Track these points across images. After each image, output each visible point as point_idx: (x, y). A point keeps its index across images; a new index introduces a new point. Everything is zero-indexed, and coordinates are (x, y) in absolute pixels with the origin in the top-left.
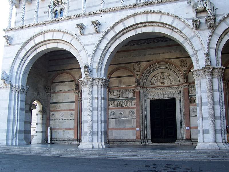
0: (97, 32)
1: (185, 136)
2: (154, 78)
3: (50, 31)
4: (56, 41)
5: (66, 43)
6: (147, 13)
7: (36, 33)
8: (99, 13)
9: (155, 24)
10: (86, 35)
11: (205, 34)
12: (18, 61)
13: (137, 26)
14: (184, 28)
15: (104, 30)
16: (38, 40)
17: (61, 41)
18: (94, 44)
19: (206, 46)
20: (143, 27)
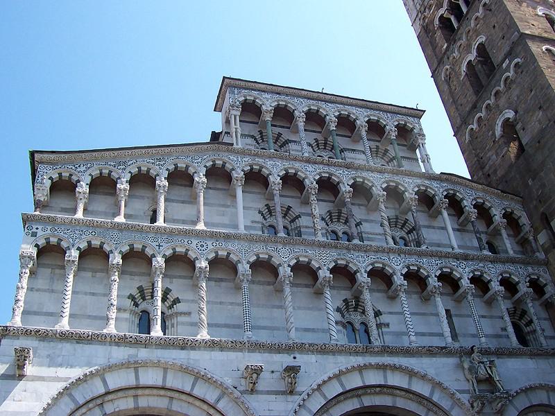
0: (291, 393)
3: (157, 364)
4: (169, 394)
5: (198, 403)
6: (383, 368)
7: (113, 361)
8: (290, 349)
10: (262, 393)
14: (452, 408)
15: (303, 385)
17: (184, 397)
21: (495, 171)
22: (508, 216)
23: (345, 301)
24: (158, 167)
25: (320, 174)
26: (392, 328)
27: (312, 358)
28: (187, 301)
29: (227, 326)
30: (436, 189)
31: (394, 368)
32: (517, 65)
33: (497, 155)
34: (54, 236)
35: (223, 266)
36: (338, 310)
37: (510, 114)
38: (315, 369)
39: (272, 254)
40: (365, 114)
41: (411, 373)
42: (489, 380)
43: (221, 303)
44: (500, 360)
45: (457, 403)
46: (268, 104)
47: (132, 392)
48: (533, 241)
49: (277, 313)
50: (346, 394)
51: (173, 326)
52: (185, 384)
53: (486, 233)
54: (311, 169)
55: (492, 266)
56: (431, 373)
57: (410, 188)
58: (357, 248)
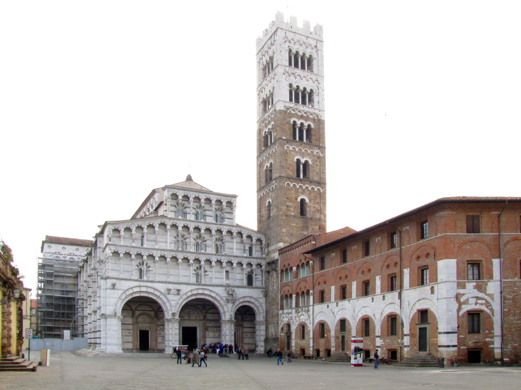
0: (178, 294)
2: (185, 314)
13: (198, 294)
15: (181, 293)
18: (176, 301)
20: (200, 295)
21: (263, 217)
22: (259, 240)
23: (197, 268)
26: (209, 276)
27: (184, 286)
31: (206, 289)
32: (276, 185)
35: (163, 257)
36: (195, 270)
37: (271, 202)
38: (185, 289)
41: (211, 291)
44: (238, 289)
49: (177, 271)
53: (250, 244)
56: (217, 291)
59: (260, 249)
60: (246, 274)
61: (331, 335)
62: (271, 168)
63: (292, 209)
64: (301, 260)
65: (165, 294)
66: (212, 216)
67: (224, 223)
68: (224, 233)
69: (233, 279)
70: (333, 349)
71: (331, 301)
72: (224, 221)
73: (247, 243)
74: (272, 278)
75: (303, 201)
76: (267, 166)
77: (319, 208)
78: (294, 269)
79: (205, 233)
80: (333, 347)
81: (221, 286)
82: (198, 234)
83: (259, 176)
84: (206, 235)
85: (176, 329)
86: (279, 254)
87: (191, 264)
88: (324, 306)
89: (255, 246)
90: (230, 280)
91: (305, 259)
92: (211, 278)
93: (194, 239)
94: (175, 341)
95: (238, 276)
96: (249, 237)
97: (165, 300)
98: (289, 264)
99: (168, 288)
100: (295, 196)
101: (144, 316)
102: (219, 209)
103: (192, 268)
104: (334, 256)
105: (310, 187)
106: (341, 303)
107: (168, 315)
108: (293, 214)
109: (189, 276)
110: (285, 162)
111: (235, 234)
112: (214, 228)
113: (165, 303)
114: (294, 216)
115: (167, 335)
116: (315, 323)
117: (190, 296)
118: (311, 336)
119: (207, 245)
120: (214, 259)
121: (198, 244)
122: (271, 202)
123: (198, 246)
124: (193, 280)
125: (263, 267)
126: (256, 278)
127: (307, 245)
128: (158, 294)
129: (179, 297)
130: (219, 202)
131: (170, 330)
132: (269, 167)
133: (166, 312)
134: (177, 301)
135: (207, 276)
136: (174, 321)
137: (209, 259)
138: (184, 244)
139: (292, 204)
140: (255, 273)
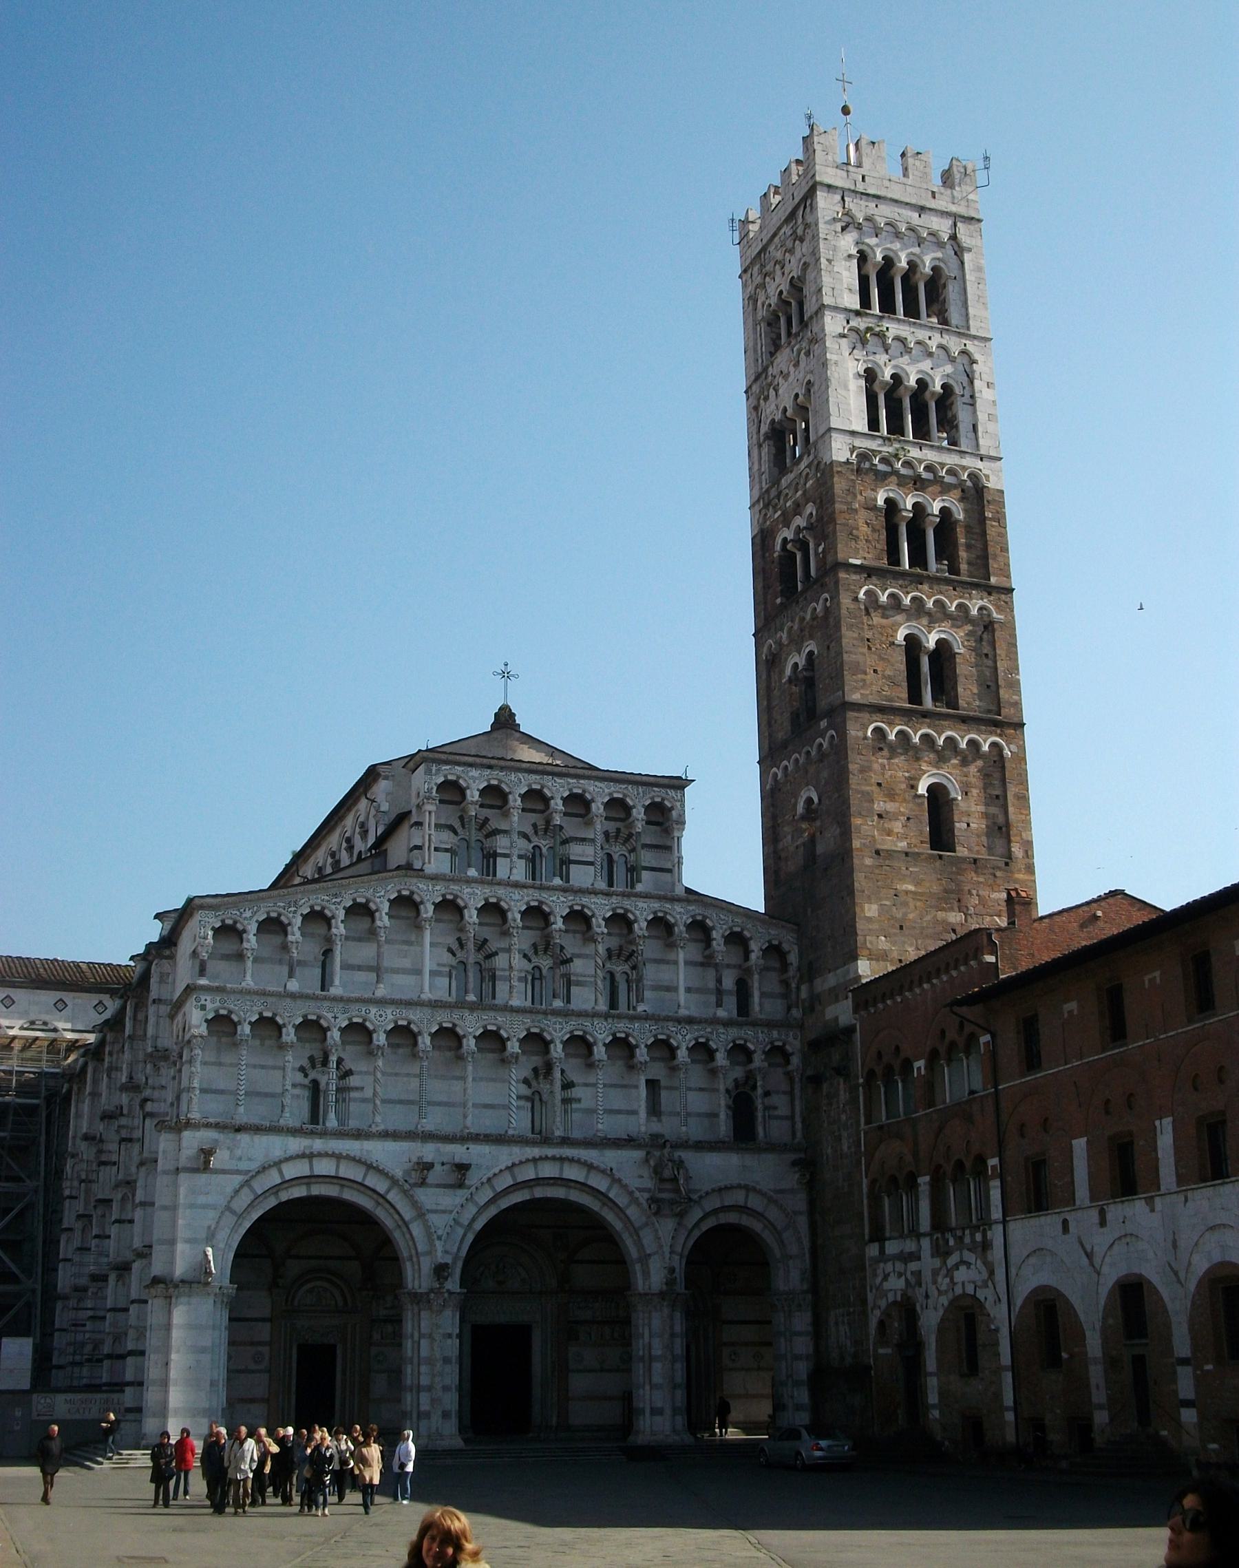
0: (461, 1185)
1: (554, 1419)
5: (370, 1193)
7: (289, 1153)
9: (572, 1184)
10: (431, 1186)
11: (667, 1226)
12: (230, 1219)
13: (539, 1181)
14: (628, 1206)
15: (473, 1178)
16: (291, 1171)
17: (355, 1186)
18: (451, 1212)
19: (667, 1250)
20: (548, 1184)
22: (774, 951)
23: (535, 1070)
24: (333, 907)
25: (528, 903)
27: (486, 1149)
28: (360, 1073)
29: (401, 1102)
30: (678, 916)
33: (793, 838)
34: (225, 1008)
35: (404, 1034)
36: (526, 1081)
37: (816, 800)
39: (457, 1022)
40: (606, 791)
41: (590, 1167)
42: (675, 1180)
43: (396, 1074)
44: (698, 1155)
45: (634, 1201)
46: (475, 782)
47: (306, 1180)
48: (794, 990)
49: (457, 1086)
50: (517, 1186)
51: (344, 1100)
52: (354, 1172)
53: (740, 967)
54: (517, 897)
55: (722, 1031)
57: (642, 912)
58: (556, 1013)
59: (777, 989)
60: (727, 1091)
61: (1086, 1354)
62: (813, 670)
63: (897, 827)
64: (943, 1032)
65: (407, 1187)
66: (591, 863)
67: (639, 888)
68: (640, 927)
69: (679, 1114)
70: (1101, 1418)
71: (1078, 1203)
72: (639, 881)
73: (728, 966)
74: (831, 1104)
75: (936, 792)
76: (796, 665)
77: (1001, 820)
78: (919, 1069)
79: (566, 931)
80: (1101, 1407)
81: (629, 1142)
82: (538, 933)
83: (765, 703)
84: (571, 935)
85: (450, 1336)
86: (856, 1009)
87: (512, 1055)
88: (1048, 1223)
89: (760, 974)
90: (664, 1118)
91: (961, 1026)
92: (591, 1111)
93: (525, 956)
94: (446, 1389)
95: (697, 1102)
96: (736, 939)
97: (408, 1214)
98: (897, 1048)
99: (421, 1158)
100: (907, 774)
101: (318, 1283)
102: (617, 837)
103: (518, 1072)
104: (1075, 1012)
105: (962, 738)
106: (1115, 1211)
107: (418, 1277)
108: (902, 845)
109: (507, 1107)
110: (865, 650)
111: (680, 929)
112: (600, 909)
113: (406, 1224)
114: (907, 854)
115: (412, 1363)
116: (1019, 1302)
117: (507, 1191)
118: (1006, 1358)
119: (573, 978)
120: (601, 1033)
121: (537, 975)
122: (816, 800)
123: (537, 983)
124: (520, 1122)
125: (795, 1060)
126: (766, 1108)
127: (962, 968)
128: (381, 1186)
129: (460, 1196)
130: (618, 807)
131: (424, 1343)
132: (804, 669)
133: (408, 1264)
134: (452, 1216)
135: (575, 1106)
136: (441, 1301)
137: (580, 1033)
138: (486, 974)
139: (897, 804)
140: (763, 1086)
